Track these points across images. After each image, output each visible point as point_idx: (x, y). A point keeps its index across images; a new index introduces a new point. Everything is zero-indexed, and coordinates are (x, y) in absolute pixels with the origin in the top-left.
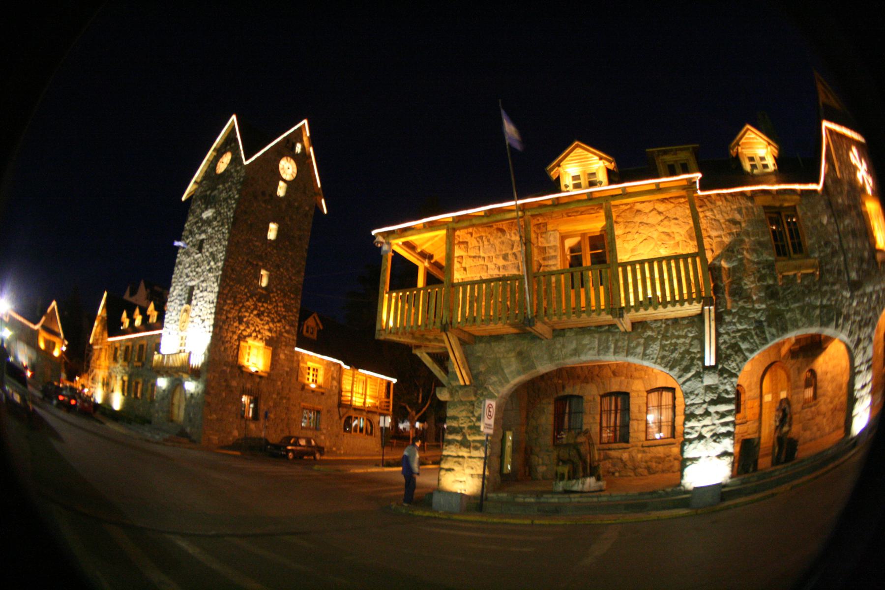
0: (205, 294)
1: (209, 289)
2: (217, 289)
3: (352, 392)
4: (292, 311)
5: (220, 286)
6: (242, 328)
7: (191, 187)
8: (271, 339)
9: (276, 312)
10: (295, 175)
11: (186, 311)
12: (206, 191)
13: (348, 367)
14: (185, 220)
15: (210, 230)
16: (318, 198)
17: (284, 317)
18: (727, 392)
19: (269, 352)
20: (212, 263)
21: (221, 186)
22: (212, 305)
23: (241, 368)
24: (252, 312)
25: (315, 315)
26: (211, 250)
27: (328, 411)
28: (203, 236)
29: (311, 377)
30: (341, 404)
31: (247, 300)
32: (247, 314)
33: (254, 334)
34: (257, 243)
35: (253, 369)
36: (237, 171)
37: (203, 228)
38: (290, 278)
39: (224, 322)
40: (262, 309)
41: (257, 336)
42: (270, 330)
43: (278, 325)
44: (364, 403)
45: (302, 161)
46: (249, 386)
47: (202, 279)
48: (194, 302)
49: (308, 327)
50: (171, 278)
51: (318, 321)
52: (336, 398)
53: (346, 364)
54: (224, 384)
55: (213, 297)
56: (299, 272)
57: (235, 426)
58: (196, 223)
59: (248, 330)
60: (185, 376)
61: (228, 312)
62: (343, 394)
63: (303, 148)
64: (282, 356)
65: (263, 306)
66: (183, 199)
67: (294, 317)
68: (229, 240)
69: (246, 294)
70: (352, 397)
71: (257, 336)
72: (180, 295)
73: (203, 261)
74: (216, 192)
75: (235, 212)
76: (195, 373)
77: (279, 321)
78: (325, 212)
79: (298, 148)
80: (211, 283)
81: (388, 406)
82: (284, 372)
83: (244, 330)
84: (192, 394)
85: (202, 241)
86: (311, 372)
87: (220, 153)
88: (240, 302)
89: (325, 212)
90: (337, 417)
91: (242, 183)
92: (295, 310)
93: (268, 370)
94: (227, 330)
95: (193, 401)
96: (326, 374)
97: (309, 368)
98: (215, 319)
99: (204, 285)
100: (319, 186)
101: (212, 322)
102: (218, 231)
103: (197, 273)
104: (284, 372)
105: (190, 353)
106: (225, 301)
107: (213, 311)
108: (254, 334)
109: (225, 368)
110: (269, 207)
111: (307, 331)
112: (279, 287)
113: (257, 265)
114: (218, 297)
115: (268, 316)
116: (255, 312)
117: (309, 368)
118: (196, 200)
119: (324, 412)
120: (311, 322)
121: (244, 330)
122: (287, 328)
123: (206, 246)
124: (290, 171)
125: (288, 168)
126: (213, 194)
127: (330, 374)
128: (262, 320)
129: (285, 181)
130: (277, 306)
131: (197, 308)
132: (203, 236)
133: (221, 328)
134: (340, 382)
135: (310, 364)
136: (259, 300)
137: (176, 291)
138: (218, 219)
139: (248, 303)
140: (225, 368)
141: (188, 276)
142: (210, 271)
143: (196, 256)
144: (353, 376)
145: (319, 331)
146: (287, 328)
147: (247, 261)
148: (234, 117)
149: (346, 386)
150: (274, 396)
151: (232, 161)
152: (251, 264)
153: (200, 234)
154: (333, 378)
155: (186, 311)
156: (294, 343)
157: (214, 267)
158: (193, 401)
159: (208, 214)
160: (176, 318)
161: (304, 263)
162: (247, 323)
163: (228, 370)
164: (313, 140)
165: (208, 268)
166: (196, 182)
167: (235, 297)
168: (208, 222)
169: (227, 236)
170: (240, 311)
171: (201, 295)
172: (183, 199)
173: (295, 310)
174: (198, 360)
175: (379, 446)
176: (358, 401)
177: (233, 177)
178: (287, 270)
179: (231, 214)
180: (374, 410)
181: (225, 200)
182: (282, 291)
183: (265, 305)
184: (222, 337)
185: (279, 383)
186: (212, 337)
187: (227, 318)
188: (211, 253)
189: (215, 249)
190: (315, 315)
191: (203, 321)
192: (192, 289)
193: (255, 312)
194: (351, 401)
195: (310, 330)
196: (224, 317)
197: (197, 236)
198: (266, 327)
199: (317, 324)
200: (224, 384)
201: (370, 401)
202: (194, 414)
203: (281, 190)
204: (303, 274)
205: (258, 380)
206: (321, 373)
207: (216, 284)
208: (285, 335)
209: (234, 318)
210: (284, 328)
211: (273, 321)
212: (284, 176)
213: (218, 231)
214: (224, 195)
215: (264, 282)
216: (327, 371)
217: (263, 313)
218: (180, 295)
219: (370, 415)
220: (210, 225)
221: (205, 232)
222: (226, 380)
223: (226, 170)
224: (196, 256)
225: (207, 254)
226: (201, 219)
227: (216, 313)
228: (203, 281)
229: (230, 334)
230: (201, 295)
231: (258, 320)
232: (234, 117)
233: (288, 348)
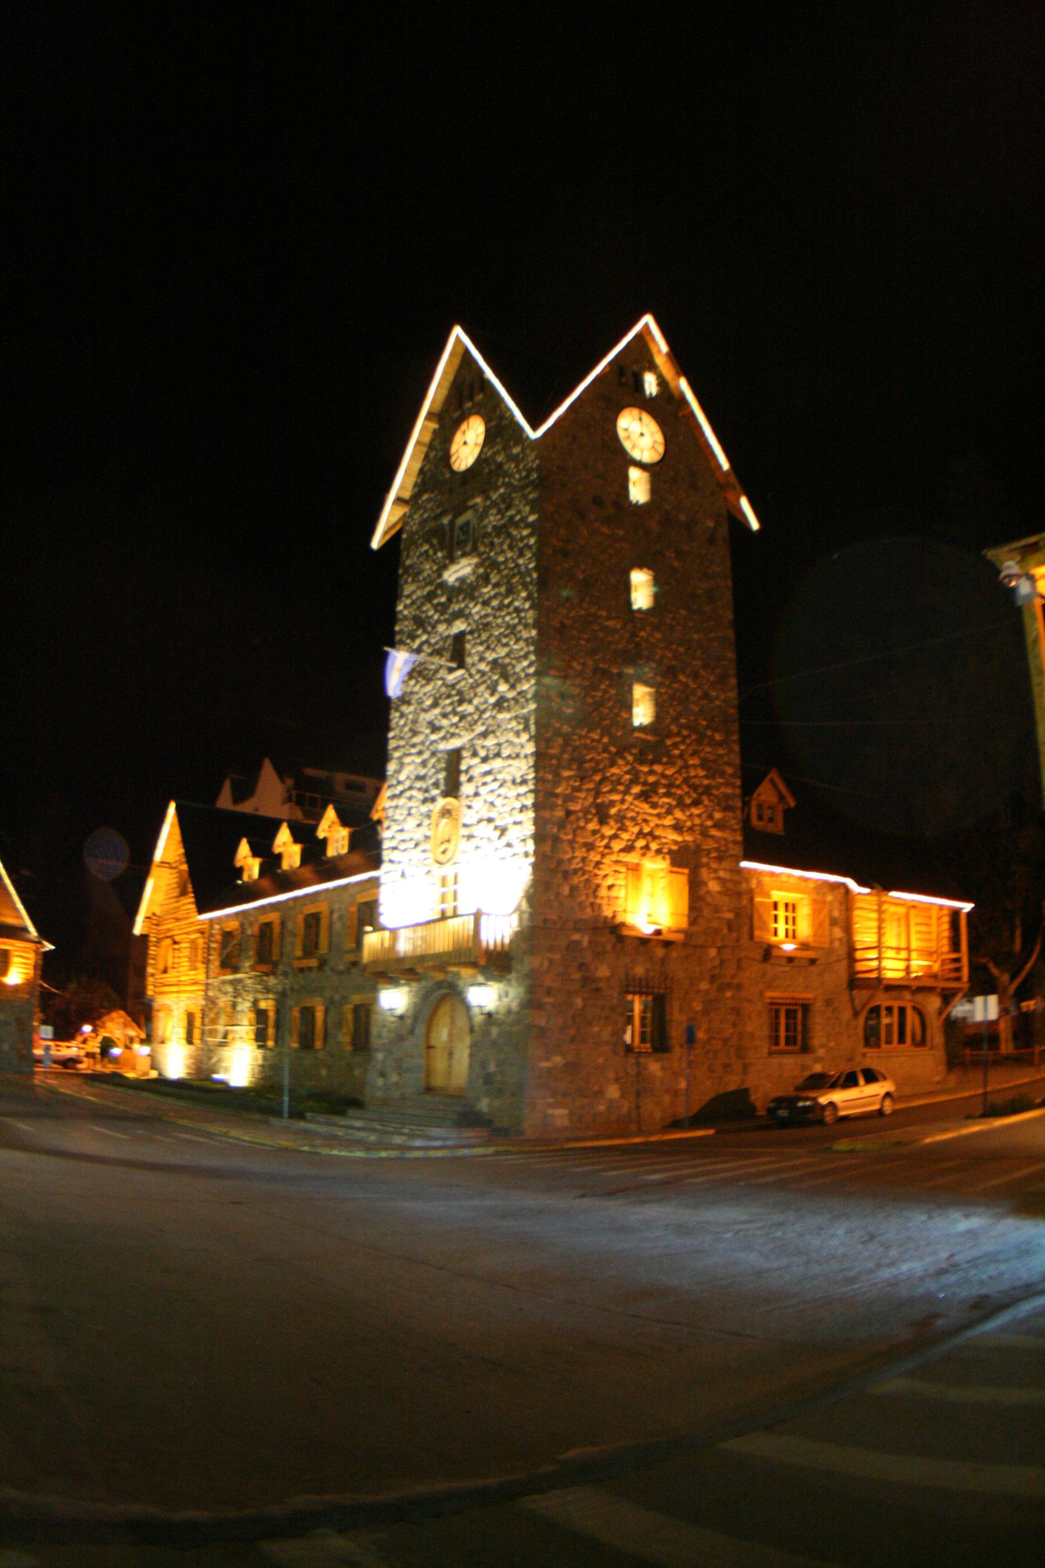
0: (497, 764)
1: (505, 753)
2: (530, 748)
3: (879, 947)
4: (722, 774)
5: (537, 739)
6: (608, 832)
7: (389, 516)
8: (684, 848)
9: (686, 781)
10: (661, 449)
11: (446, 812)
12: (437, 517)
13: (867, 890)
14: (393, 594)
15: (476, 609)
16: (731, 497)
17: (707, 790)
19: (682, 880)
20: (503, 687)
21: (478, 500)
22: (523, 789)
23: (615, 930)
24: (626, 792)
25: (774, 775)
26: (490, 656)
27: (828, 1002)
28: (460, 626)
29: (781, 926)
30: (855, 982)
31: (613, 764)
32: (616, 797)
33: (641, 843)
34: (611, 623)
35: (647, 930)
36: (516, 459)
37: (455, 607)
38: (706, 695)
39: (561, 826)
40: (651, 779)
41: (647, 847)
42: (677, 827)
43: (696, 811)
44: (907, 969)
45: (666, 410)
46: (639, 970)
47: (480, 728)
48: (467, 789)
49: (760, 806)
50: (385, 741)
51: (784, 790)
52: (842, 969)
53: (861, 883)
54: (577, 976)
55: (523, 767)
56: (722, 680)
57: (611, 1075)
58: (430, 597)
59: (625, 836)
60: (466, 972)
61: (569, 798)
62: (859, 955)
63: (662, 383)
64: (713, 886)
65: (651, 772)
66: (375, 544)
67: (732, 790)
68: (536, 625)
69: (605, 750)
70: (879, 959)
71: (647, 847)
72: (419, 778)
73: (474, 686)
74: (468, 515)
75: (539, 556)
76: (496, 963)
77: (696, 803)
78: (755, 525)
79: (650, 384)
80: (511, 736)
81: (958, 970)
82: (722, 921)
83: (615, 837)
84: (489, 1015)
85: (460, 637)
86: (781, 913)
87: (448, 423)
88: (595, 771)
89: (755, 525)
90: (847, 1015)
91: (541, 484)
92: (730, 770)
93: (684, 923)
94: (571, 843)
95: (495, 1031)
96: (816, 912)
97: (775, 906)
98: (537, 821)
99: (490, 742)
100: (725, 464)
101: (529, 829)
102: (500, 607)
103: (463, 717)
104: (722, 921)
105: (477, 916)
106: (557, 774)
107: (529, 801)
108: (641, 843)
109: (576, 937)
110: (621, 533)
111: (760, 818)
112: (683, 721)
113: (620, 675)
114: (537, 767)
115: (667, 795)
116: (636, 789)
117: (775, 906)
118: (412, 543)
119: (818, 1006)
120: (765, 794)
121: (615, 837)
122: (718, 815)
123: (473, 649)
124: (647, 442)
125: (640, 435)
126: (461, 521)
127: (825, 912)
128: (654, 806)
130: (686, 767)
131: (477, 803)
132: (460, 626)
133: (556, 840)
134: (848, 928)
135: (777, 895)
136: (641, 759)
137: (405, 767)
138: (494, 579)
139: (614, 770)
140: (576, 937)
141: (435, 728)
142: (499, 705)
143: (451, 678)
144: (880, 911)
145: (788, 813)
146: (718, 815)
147: (596, 670)
148: (458, 331)
149: (865, 936)
150: (704, 986)
151: (490, 437)
152: (605, 673)
153: (449, 623)
154: (834, 922)
155: (446, 812)
156: (737, 850)
157: (511, 695)
158: (495, 1031)
160: (418, 835)
161: (731, 655)
162: (621, 818)
163: (585, 940)
164: (680, 357)
165: (492, 700)
166: (399, 500)
167: (581, 762)
168: (466, 590)
169: (530, 616)
170: (598, 793)
171: (486, 767)
172: (375, 544)
173: (730, 770)
174: (500, 928)
175: (942, 1068)
176: (893, 969)
177: (506, 474)
178: (695, 676)
179: (527, 562)
180: (930, 983)
181: (499, 530)
182: (692, 728)
183: (658, 768)
184: (560, 862)
185: (713, 952)
186: (535, 866)
187: (569, 813)
188: (495, 663)
189: (502, 652)
190: (774, 775)
191: (503, 831)
192: (455, 756)
193: (636, 789)
194: (879, 969)
195: (767, 814)
196: (560, 813)
197: (441, 628)
198: (668, 821)
199: (781, 798)
200: (577, 976)
201: (918, 964)
202: (500, 1063)
203: (639, 489)
204: (733, 681)
205: (660, 952)
206: (804, 912)
207: (525, 737)
208: (714, 832)
209: (586, 811)
210: (710, 817)
211: (681, 805)
212: (636, 455)
213: (500, 607)
214: (493, 519)
215: (642, 713)
216: (818, 906)
217: (654, 788)
218: (419, 778)
219: (919, 998)
220: (473, 598)
221: (460, 614)
222: (582, 966)
223: (480, 461)
224: (451, 678)
225: (483, 666)
226: (443, 585)
227: (536, 806)
228: (484, 735)
229: (580, 853)
230: (486, 767)
231: (646, 807)
232: (458, 331)
233: (725, 865)
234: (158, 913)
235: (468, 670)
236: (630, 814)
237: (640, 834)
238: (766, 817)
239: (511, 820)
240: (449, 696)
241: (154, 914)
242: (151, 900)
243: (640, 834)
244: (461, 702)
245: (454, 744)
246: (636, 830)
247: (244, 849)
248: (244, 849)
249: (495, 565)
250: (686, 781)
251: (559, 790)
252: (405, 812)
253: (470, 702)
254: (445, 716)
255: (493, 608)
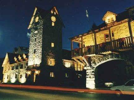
0: (39, 50)
3: (77, 67)
7: (30, 26)
18: (94, 62)
28: (36, 37)
48: (36, 53)
63: (56, 13)
98: (42, 56)
114: (42, 51)
124: (54, 20)
132: (36, 37)
142: (39, 45)
155: (34, 55)
159: (36, 32)
168: (36, 34)
203: (53, 24)
212: (53, 21)
228: (38, 48)
245: (35, 49)
247: (15, 58)
248: (15, 58)
249: (39, 32)
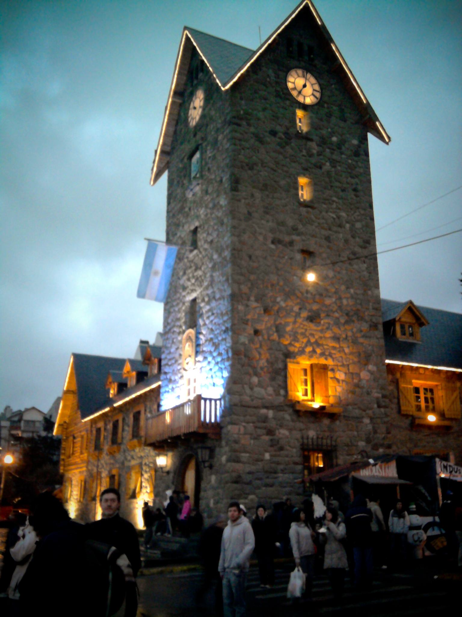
1: (218, 296)
26: (209, 239)
33: (309, 349)
41: (314, 351)
71: (314, 351)
97: (417, 390)
108: (309, 349)
111: (403, 333)
124: (308, 90)
129: (304, 107)
135: (417, 383)
143: (191, 256)
150: (362, 444)
193: (304, 314)
197: (186, 227)
198: (328, 334)
208: (361, 340)
211: (337, 323)
223: (203, 117)
234: (67, 421)
235: (199, 250)
236: (300, 331)
237: (309, 343)
238: (407, 333)
239: (220, 338)
240: (191, 267)
241: (65, 422)
242: (62, 414)
243: (309, 343)
244: (196, 270)
246: (305, 340)
250: (340, 307)
251: (249, 317)
252: (171, 342)
253: (200, 268)
254: (189, 280)
255: (210, 209)
